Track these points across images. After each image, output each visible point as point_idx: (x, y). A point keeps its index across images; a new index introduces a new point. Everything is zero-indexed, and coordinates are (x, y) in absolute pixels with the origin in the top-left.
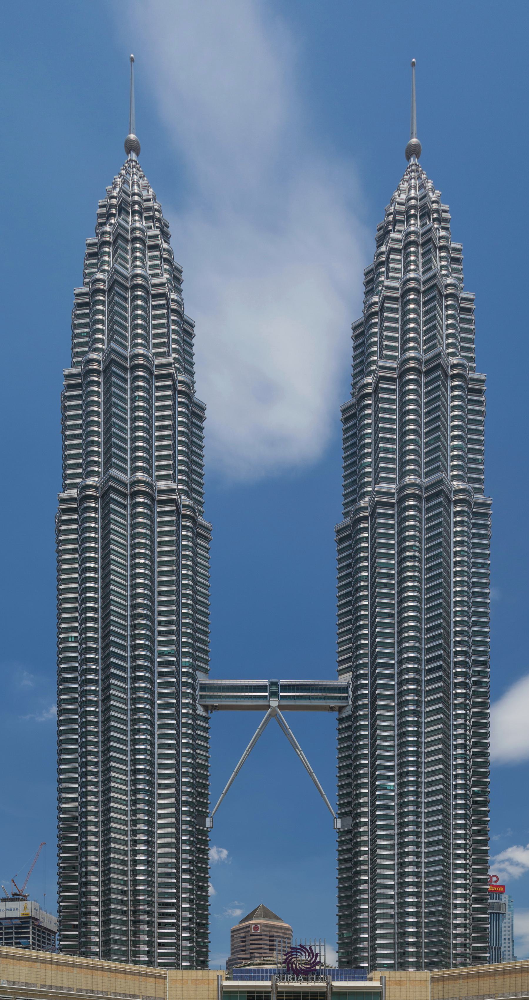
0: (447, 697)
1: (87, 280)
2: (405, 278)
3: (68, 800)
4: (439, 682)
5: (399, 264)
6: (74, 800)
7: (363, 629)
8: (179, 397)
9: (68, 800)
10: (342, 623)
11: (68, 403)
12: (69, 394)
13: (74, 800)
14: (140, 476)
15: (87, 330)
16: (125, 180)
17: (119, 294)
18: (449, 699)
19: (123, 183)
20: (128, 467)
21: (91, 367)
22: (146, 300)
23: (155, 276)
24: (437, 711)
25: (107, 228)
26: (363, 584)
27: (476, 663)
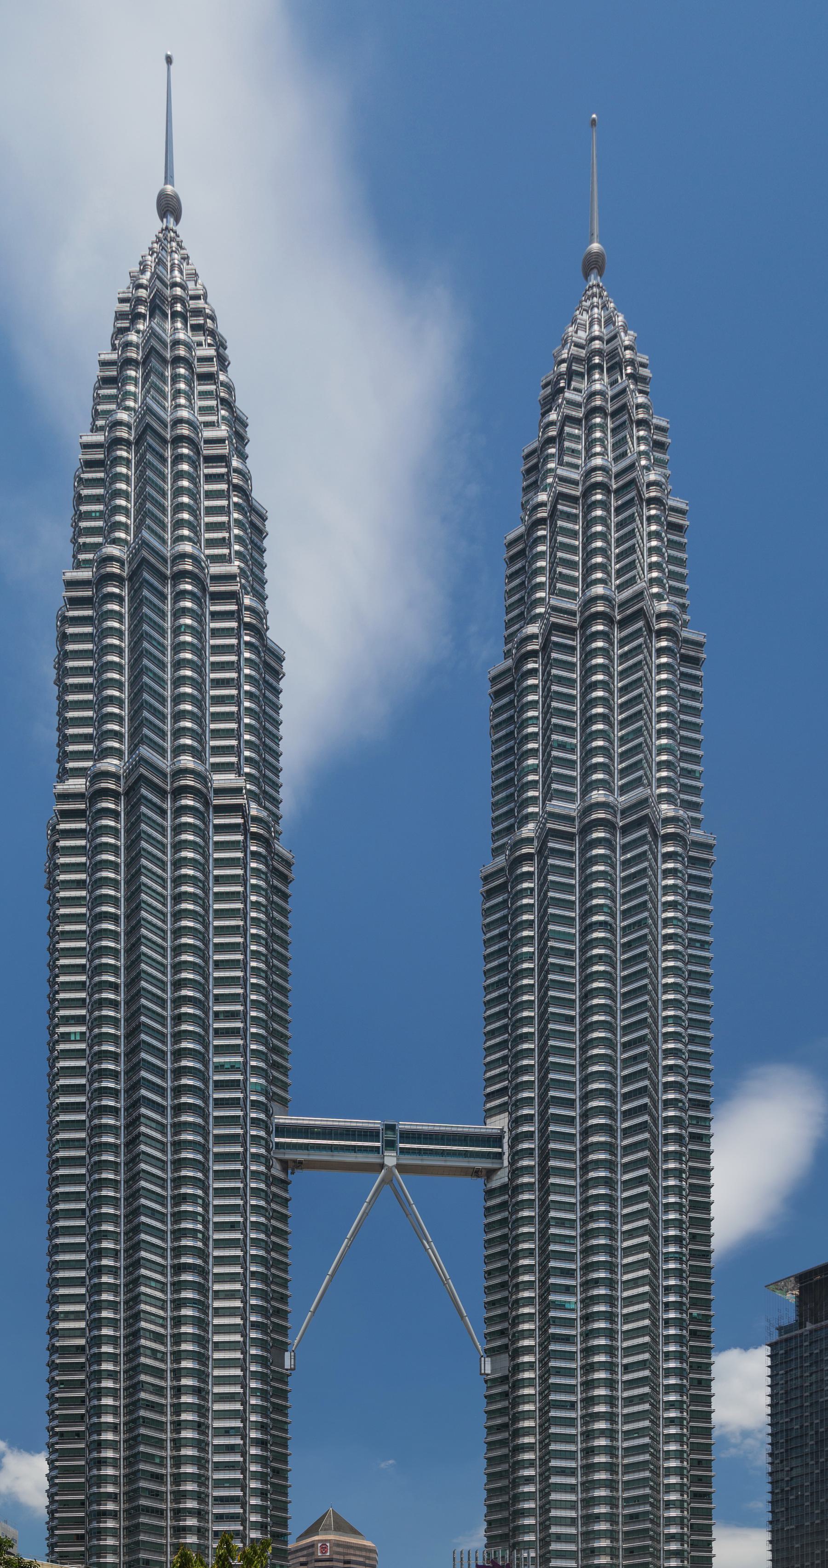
1: (100, 423)
8: (246, 634)
11: (71, 630)
12: (71, 614)
14: (187, 761)
15: (101, 507)
16: (160, 259)
17: (154, 450)
19: (158, 264)
20: (168, 745)
21: (108, 569)
22: (194, 464)
23: (208, 424)
25: (133, 337)
26: (525, 965)
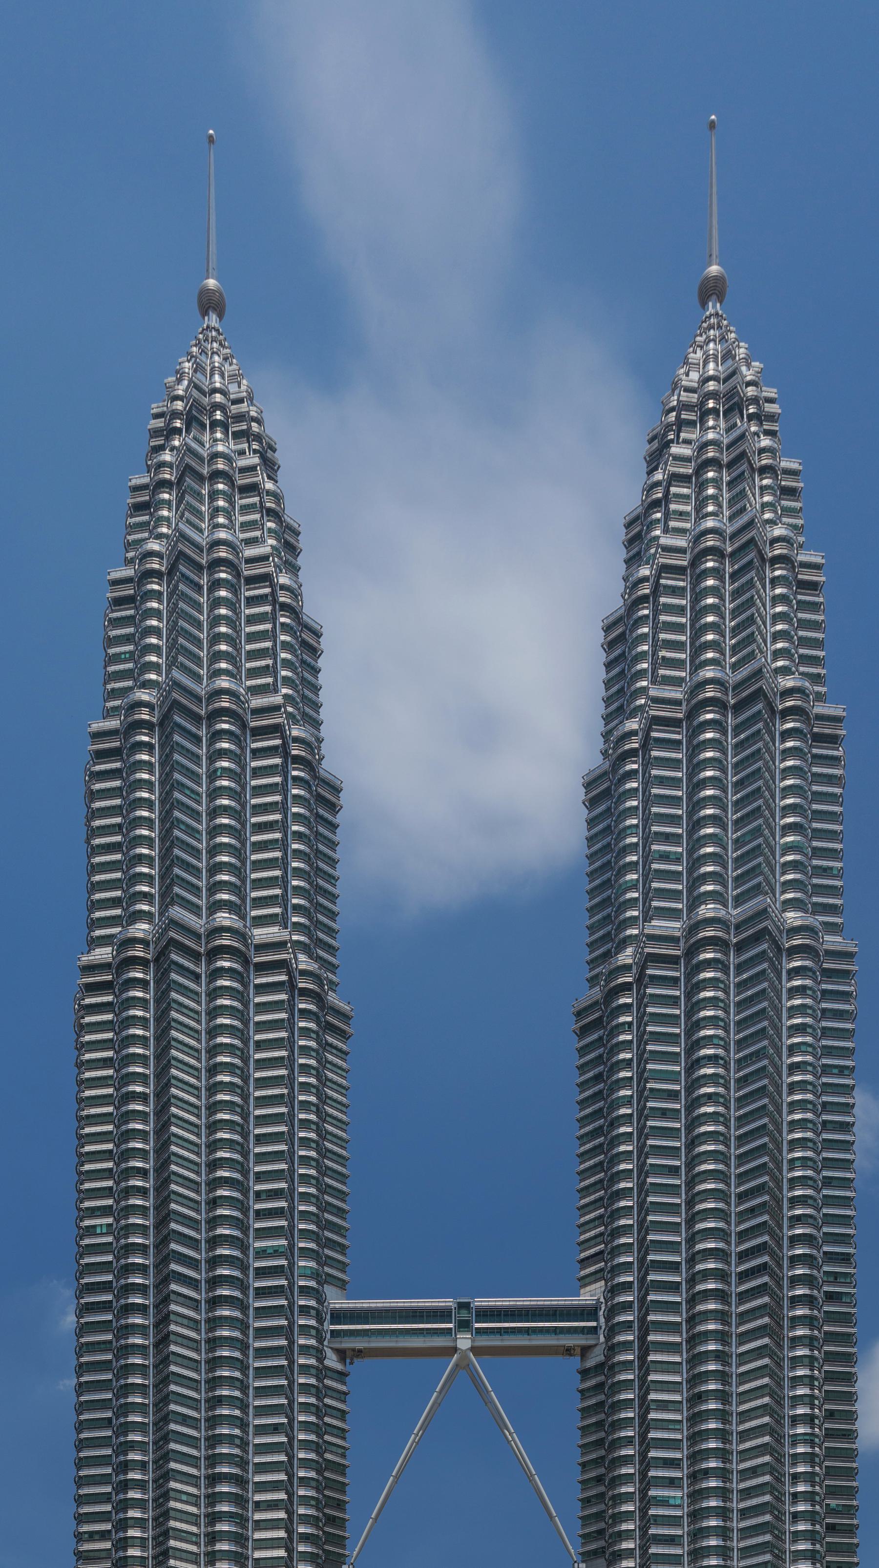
0: (778, 1324)
2: (697, 530)
3: (92, 1536)
4: (762, 1296)
5: (687, 504)
6: (103, 1535)
7: (624, 1198)
9: (92, 1536)
10: (586, 1188)
13: (103, 1535)
18: (781, 1327)
24: (758, 1353)
27: (830, 1257)
